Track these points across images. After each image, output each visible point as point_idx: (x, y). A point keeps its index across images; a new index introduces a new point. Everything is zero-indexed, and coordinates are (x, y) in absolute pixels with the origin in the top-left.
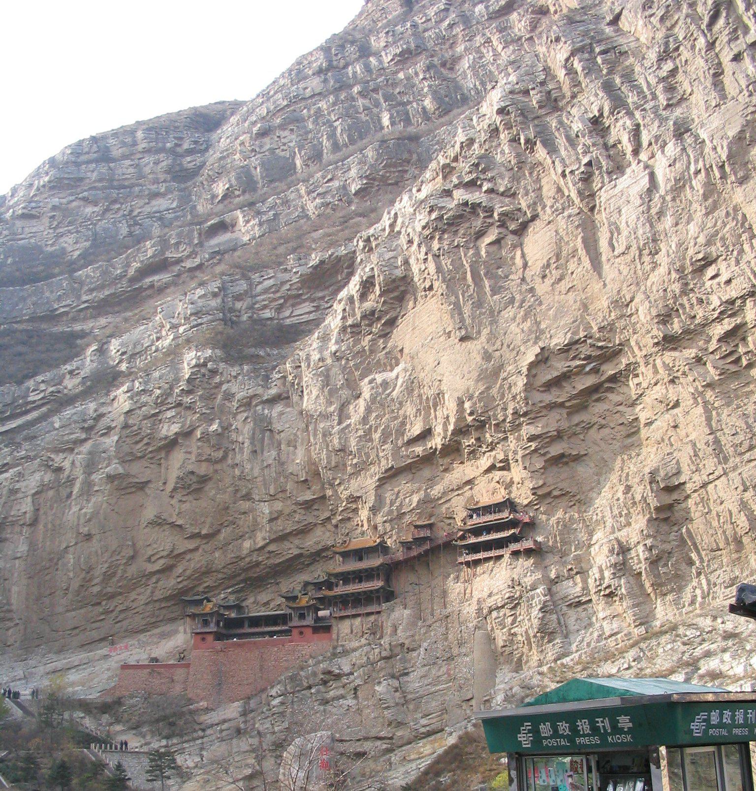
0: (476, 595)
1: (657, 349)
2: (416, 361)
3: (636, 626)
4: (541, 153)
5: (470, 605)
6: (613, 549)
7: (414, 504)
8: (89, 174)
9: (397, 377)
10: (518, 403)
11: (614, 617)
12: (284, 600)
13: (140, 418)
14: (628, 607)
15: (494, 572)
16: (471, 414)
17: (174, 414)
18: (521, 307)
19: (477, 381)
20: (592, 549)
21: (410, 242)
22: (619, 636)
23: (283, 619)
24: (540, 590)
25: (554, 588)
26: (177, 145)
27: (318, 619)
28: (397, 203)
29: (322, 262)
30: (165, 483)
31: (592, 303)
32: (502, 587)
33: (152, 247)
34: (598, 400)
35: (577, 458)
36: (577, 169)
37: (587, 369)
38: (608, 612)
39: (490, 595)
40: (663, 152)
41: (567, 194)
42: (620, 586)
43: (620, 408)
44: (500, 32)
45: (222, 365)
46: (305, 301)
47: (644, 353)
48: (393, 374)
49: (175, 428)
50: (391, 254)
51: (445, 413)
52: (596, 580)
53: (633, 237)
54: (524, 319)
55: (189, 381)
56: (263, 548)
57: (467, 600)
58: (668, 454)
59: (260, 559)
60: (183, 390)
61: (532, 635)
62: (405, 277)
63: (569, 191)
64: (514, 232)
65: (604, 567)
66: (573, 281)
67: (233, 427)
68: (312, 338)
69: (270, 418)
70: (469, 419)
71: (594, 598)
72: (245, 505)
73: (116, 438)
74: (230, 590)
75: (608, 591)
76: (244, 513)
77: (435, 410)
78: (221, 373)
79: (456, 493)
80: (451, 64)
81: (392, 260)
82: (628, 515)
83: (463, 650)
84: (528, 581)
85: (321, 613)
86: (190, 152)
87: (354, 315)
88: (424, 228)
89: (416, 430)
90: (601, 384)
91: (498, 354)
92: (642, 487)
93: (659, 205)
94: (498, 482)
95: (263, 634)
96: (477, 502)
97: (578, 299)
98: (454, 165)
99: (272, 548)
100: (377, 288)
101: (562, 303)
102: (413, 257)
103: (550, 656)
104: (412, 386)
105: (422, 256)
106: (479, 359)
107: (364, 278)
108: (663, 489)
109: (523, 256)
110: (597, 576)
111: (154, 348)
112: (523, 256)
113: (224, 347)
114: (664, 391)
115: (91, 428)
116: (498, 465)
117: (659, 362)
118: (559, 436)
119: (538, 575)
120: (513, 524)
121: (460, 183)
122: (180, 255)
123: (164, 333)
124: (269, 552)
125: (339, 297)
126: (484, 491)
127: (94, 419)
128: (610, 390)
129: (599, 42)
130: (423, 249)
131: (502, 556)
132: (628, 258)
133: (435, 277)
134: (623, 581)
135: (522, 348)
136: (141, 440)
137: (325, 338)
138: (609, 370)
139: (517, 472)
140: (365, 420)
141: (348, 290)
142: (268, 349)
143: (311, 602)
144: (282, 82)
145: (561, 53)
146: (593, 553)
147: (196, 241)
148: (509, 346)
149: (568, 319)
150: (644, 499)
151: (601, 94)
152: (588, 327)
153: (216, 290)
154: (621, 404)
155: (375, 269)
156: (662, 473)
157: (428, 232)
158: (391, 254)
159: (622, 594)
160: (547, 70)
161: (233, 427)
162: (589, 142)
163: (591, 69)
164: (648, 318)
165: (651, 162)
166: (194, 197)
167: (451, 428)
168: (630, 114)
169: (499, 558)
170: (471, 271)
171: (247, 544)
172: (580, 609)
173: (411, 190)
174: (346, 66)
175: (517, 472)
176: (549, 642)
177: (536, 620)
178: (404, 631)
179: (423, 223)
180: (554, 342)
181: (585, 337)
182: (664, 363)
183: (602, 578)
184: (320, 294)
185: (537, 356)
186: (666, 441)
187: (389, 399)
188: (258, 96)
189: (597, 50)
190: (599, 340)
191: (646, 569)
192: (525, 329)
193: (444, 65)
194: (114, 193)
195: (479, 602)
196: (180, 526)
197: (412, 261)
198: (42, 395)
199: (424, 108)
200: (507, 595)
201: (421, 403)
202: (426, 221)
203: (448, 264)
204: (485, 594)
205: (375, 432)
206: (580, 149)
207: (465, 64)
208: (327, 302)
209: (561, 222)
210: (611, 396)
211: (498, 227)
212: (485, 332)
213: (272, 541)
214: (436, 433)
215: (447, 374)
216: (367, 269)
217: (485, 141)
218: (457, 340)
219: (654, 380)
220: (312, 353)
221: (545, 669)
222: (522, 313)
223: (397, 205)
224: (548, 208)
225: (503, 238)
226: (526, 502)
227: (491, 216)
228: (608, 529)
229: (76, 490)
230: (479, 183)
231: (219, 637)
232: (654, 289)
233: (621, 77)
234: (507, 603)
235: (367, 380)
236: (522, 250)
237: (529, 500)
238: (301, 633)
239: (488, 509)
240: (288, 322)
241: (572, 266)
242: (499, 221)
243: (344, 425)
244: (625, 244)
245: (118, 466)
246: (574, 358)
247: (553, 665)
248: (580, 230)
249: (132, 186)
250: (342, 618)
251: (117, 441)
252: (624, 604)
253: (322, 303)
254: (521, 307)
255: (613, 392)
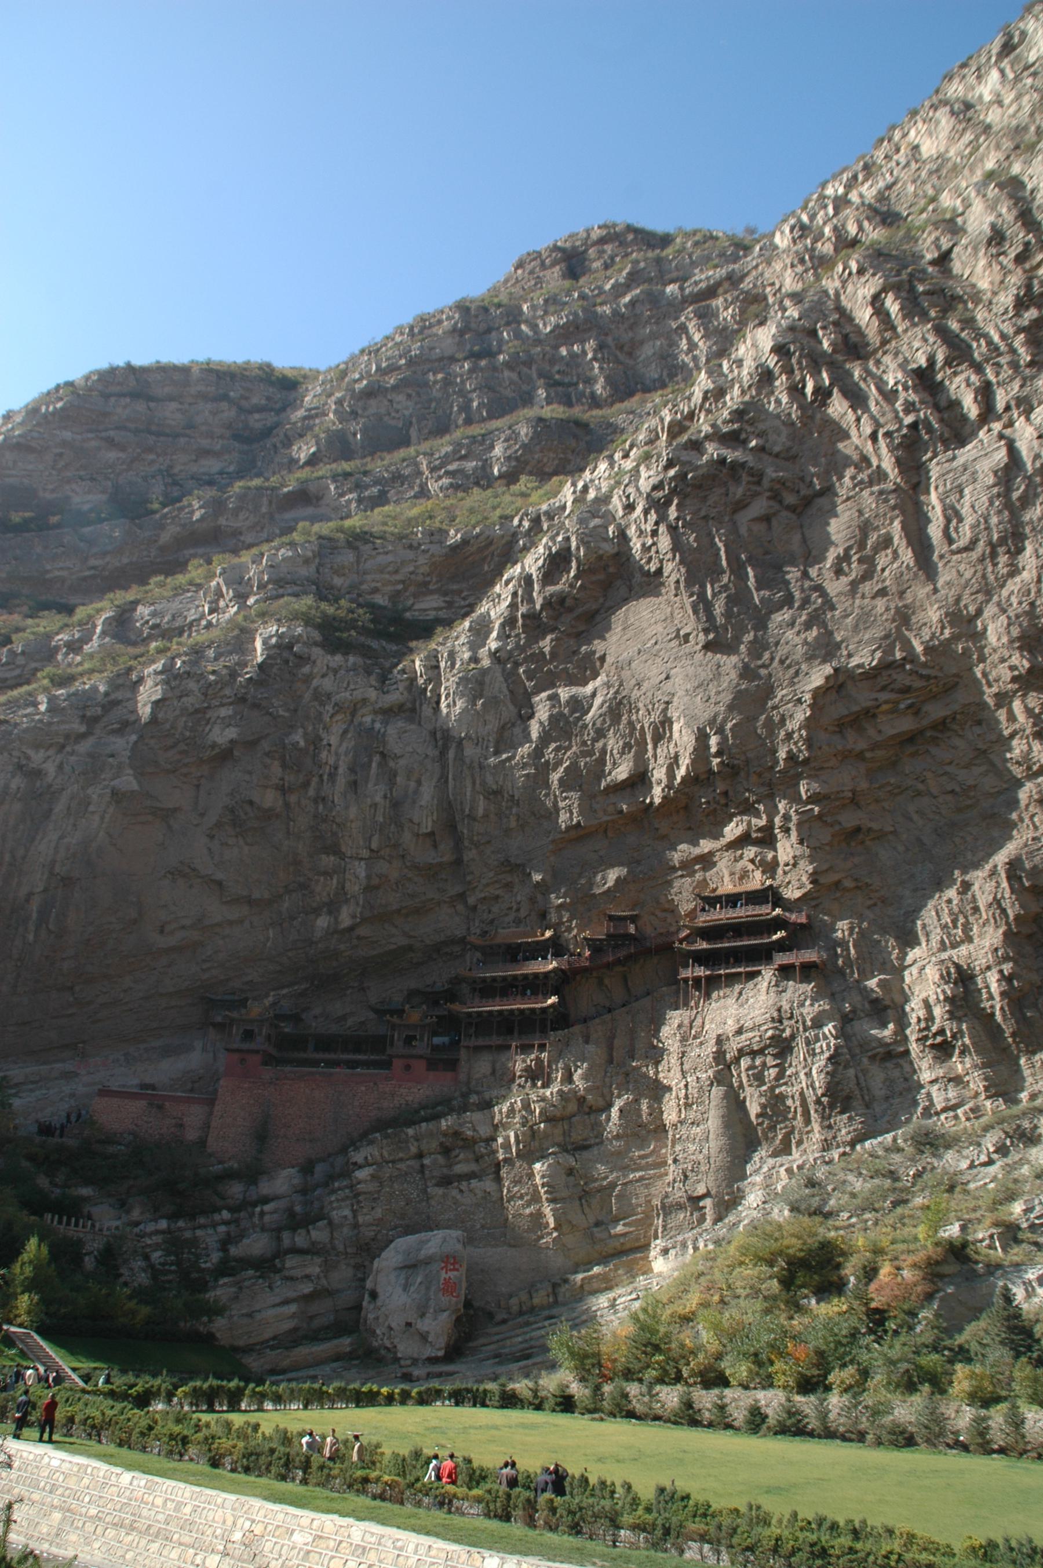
0: (712, 1030)
1: (1016, 686)
2: (626, 674)
3: (988, 1098)
4: (838, 407)
5: (701, 1043)
6: (949, 973)
7: (610, 883)
8: (119, 410)
9: (594, 695)
10: (795, 743)
11: (950, 1080)
12: (372, 1015)
13: (177, 712)
14: (975, 1066)
15: (744, 996)
16: (719, 754)
17: (230, 712)
18: (802, 607)
19: (731, 708)
20: (906, 973)
21: (630, 507)
22: (960, 1111)
23: (379, 1043)
24: (829, 1028)
25: (848, 1028)
26: (243, 397)
27: (435, 1048)
28: (587, 472)
29: (465, 542)
30: (202, 815)
31: (914, 613)
32: (759, 1020)
33: (200, 507)
34: (913, 755)
35: (880, 836)
36: (898, 430)
37: (902, 706)
38: (941, 1072)
39: (739, 1032)
40: (1028, 419)
41: (875, 463)
42: (961, 1031)
43: (948, 768)
44: (699, 318)
45: (317, 652)
46: (432, 592)
47: (995, 689)
48: (589, 688)
49: (232, 733)
50: (597, 521)
51: (672, 751)
52: (919, 1020)
53: (982, 527)
54: (808, 626)
55: (261, 666)
56: (351, 929)
57: (695, 1037)
58: (1034, 839)
59: (342, 947)
60: (251, 678)
61: (811, 1099)
62: (617, 554)
63: (880, 460)
64: (792, 509)
65: (932, 1000)
66: (884, 581)
67: (325, 742)
68: (460, 629)
69: (384, 735)
70: (716, 761)
71: (914, 1047)
72: (328, 861)
73: (134, 738)
74: (285, 991)
75: (939, 1039)
76: (325, 873)
77: (655, 748)
78: (314, 662)
79: (680, 873)
80: (631, 349)
81: (600, 530)
82: (967, 927)
83: (692, 1115)
84: (809, 1011)
85: (437, 1040)
86: (259, 409)
87: (531, 601)
88: (655, 488)
89: (622, 772)
90: (921, 732)
91: (763, 672)
92: (993, 884)
93: (1023, 487)
94: (752, 861)
95: (336, 1064)
96: (714, 890)
97: (892, 606)
98: (687, 423)
99: (362, 931)
100: (574, 564)
101: (867, 610)
102: (633, 528)
103: (844, 1134)
104: (616, 709)
105: (649, 527)
106: (734, 675)
107: (554, 550)
108: (1026, 889)
109: (804, 540)
110: (922, 1013)
111: (204, 623)
112: (804, 540)
113: (319, 627)
114: (1025, 748)
115: (96, 719)
116: (754, 835)
117: (1017, 705)
118: (855, 801)
119: (824, 1005)
120: (778, 924)
121: (715, 434)
122: (239, 525)
123: (222, 604)
124: (359, 938)
125: (505, 578)
126: (726, 873)
127: (103, 707)
128: (935, 740)
129: (922, 281)
130: (653, 517)
131: (759, 973)
132: (975, 555)
133: (669, 556)
134: (964, 1026)
135: (804, 667)
136: (172, 747)
137: (481, 631)
138: (936, 711)
139: (786, 849)
140: (538, 753)
141: (523, 568)
142: (384, 643)
143: (428, 1020)
144: (398, 339)
145: (865, 289)
146: (908, 979)
147: (264, 510)
148: (782, 662)
149: (878, 632)
150: (997, 902)
151: (931, 340)
152: (907, 645)
153: (310, 554)
154: (950, 763)
155: (573, 539)
156: (1028, 865)
157: (661, 494)
158: (597, 521)
159: (964, 1045)
160: (839, 309)
161: (325, 742)
162: (913, 397)
163: (913, 309)
164: (1005, 640)
165: (1007, 432)
166: (259, 464)
167: (681, 772)
168: (978, 369)
169: (752, 976)
170: (726, 552)
171: (322, 922)
172: (889, 1065)
173: (611, 457)
174: (489, 331)
175: (786, 849)
176: (842, 1112)
177: (823, 1076)
178: (585, 1077)
179: (654, 481)
180: (854, 662)
181: (904, 659)
182: (1026, 707)
183: (930, 1018)
184: (455, 587)
185: (827, 678)
186: (1027, 821)
187: (580, 723)
188: (362, 351)
189: (921, 289)
190: (925, 665)
191: (1002, 1008)
192: (809, 639)
193: (621, 348)
194: (151, 440)
195: (720, 1040)
196: (219, 883)
197: (632, 532)
198: (17, 672)
199: (593, 395)
200: (770, 1033)
201: (631, 734)
202: (659, 478)
203: (692, 539)
204: (731, 1026)
205: (554, 769)
206: (899, 405)
207: (647, 351)
208: (464, 599)
209: (868, 499)
210: (934, 750)
211: (769, 498)
212: (749, 637)
213: (364, 920)
214: (653, 780)
215: (681, 693)
216: (560, 538)
217: (750, 387)
218: (699, 647)
219: (1009, 731)
220: (457, 648)
221: (835, 1154)
222: (804, 618)
223: (587, 475)
224: (847, 480)
225: (775, 514)
226: (797, 894)
227: (759, 483)
228: (935, 943)
229: (59, 807)
230: (743, 436)
231: (269, 1060)
232: (1014, 600)
233: (959, 321)
234: (770, 1046)
235: (544, 695)
236: (803, 534)
237: (803, 891)
238: (408, 1067)
239: (732, 900)
240: (408, 615)
241: (882, 559)
242: (771, 490)
243: (504, 756)
244: (969, 534)
245: (131, 778)
246: (883, 689)
247: (848, 1149)
248: (897, 512)
249: (177, 436)
250: (478, 1049)
251: (136, 743)
252: (967, 1059)
253: (457, 598)
254: (802, 607)
255: (938, 745)
